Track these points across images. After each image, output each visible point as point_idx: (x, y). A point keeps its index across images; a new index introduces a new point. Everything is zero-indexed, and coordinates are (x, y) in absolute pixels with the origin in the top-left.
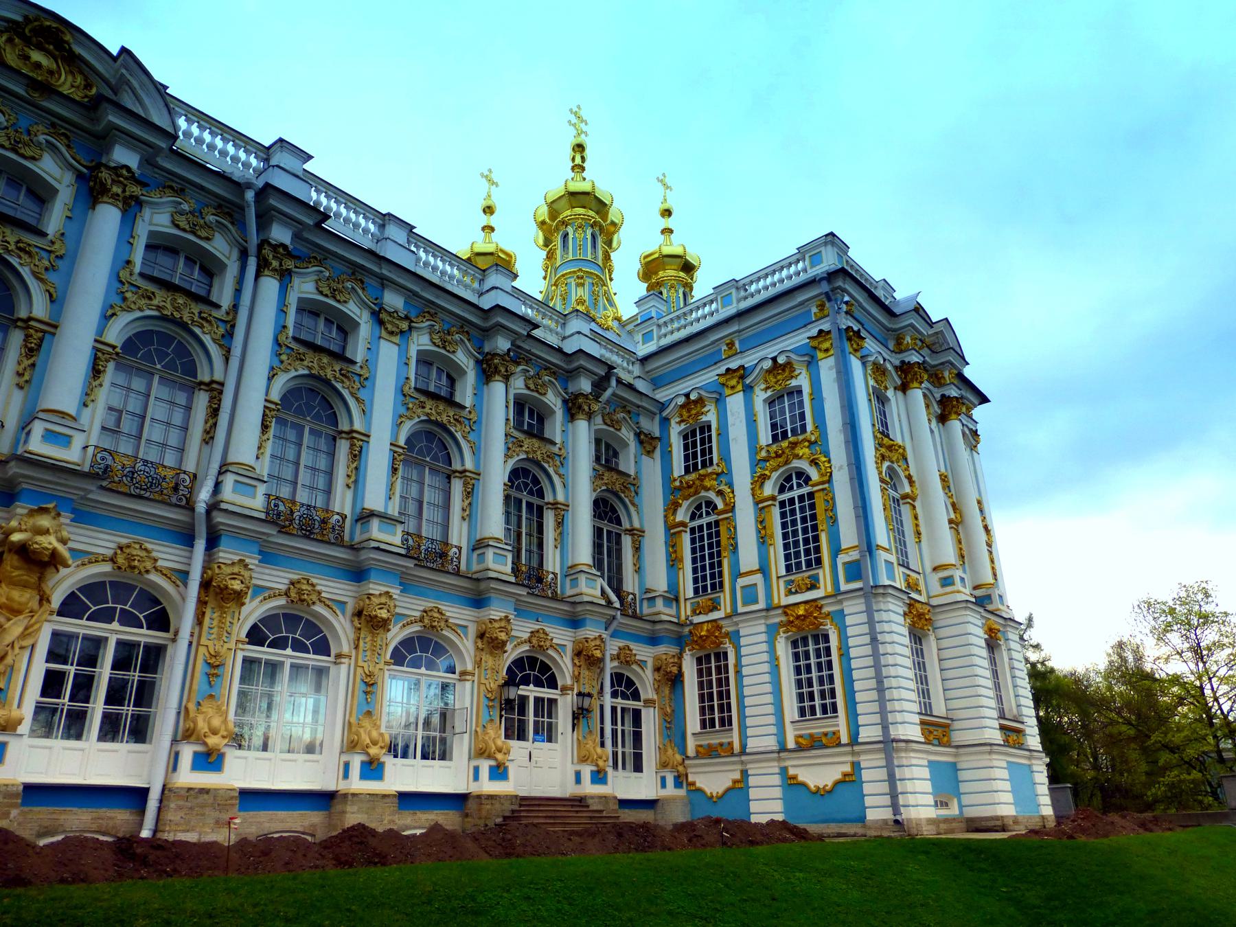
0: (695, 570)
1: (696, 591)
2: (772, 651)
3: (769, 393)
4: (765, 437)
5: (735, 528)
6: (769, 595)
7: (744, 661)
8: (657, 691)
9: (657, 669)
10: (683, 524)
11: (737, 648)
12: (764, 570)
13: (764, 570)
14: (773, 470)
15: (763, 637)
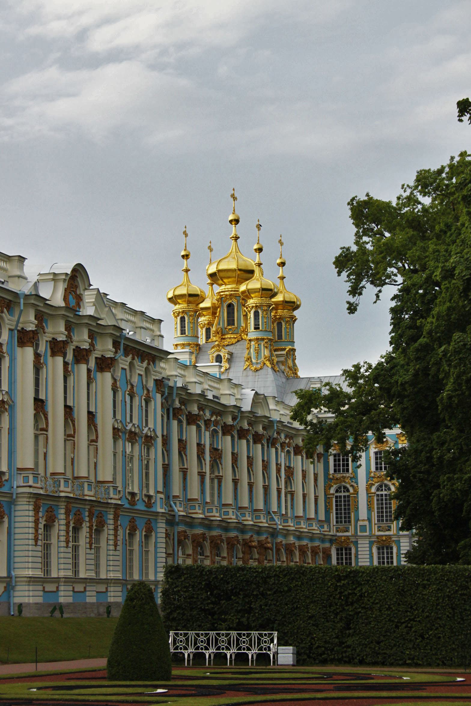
0: (337, 514)
1: (337, 522)
2: (371, 550)
3: (376, 450)
4: (373, 468)
5: (358, 501)
6: (371, 529)
7: (359, 553)
8: (323, 561)
9: (324, 553)
10: (333, 494)
11: (357, 548)
12: (369, 520)
13: (369, 520)
14: (375, 482)
15: (368, 545)
